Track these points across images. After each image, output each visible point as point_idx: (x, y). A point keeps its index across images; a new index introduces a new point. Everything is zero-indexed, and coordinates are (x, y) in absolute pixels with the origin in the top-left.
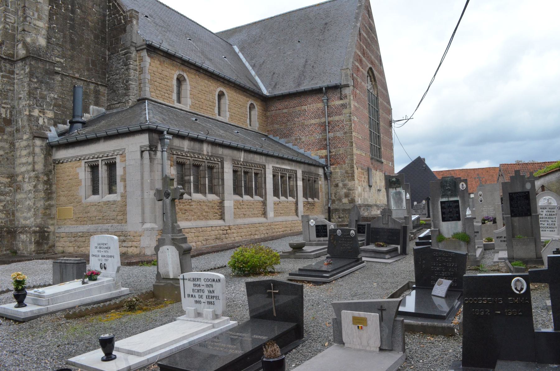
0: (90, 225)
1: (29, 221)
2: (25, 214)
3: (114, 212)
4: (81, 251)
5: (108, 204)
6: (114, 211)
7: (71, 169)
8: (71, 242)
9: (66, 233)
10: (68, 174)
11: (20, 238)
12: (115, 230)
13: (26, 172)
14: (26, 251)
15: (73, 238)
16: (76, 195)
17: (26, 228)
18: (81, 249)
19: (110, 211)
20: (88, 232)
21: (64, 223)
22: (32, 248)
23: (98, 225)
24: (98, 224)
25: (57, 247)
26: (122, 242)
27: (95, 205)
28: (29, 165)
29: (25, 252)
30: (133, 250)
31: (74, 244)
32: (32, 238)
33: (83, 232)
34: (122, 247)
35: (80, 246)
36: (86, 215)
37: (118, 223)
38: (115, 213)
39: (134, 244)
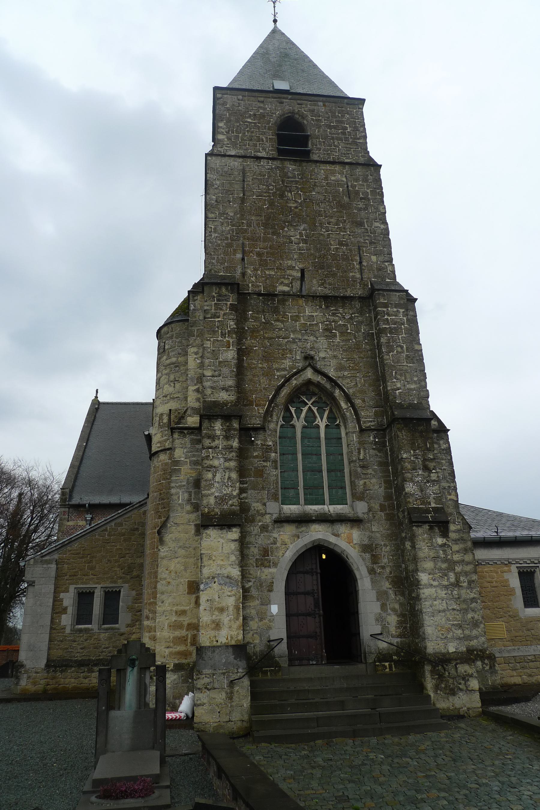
1: (475, 641)
7: (495, 574)
10: (489, 579)
13: (461, 573)
16: (508, 607)
22: (496, 680)
28: (467, 565)
33: (534, 655)
35: (533, 674)
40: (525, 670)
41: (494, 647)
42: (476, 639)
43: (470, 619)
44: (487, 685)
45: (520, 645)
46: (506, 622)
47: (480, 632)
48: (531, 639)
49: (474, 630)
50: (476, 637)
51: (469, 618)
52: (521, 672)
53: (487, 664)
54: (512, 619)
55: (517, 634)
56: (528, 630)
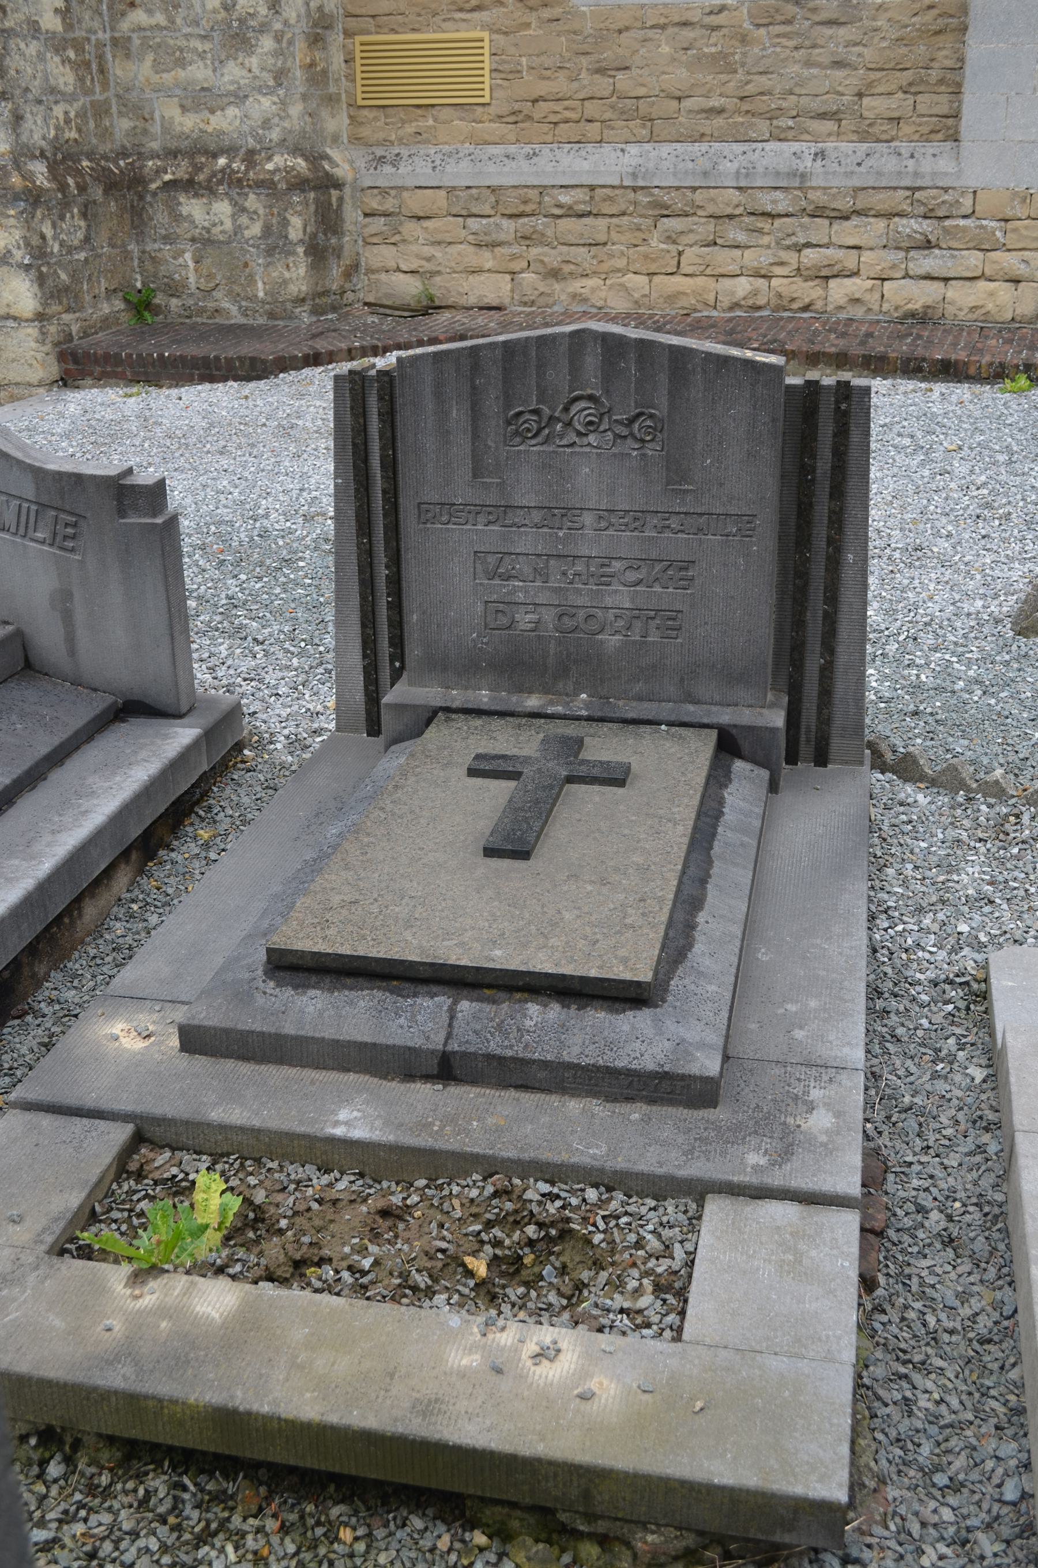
0: (633, 149)
1: (232, 111)
2: (199, 72)
3: (840, 74)
4: (574, 296)
5: (788, 22)
6: (838, 64)
8: (494, 245)
9: (451, 190)
11: (177, 217)
12: (857, 182)
14: (235, 298)
15: (505, 223)
17: (215, 156)
18: (575, 286)
19: (808, 64)
20: (635, 189)
21: (410, 129)
22: (285, 282)
23: (704, 147)
24: (701, 137)
25: (370, 271)
26: (908, 249)
27: (685, 24)
29: (226, 304)
30: (991, 294)
31: (514, 257)
32: (285, 223)
33: (592, 188)
34: (907, 276)
35: (567, 268)
36: (602, 85)
37: (864, 136)
38: (848, 81)
39: (1010, 261)
40: (535, 251)
41: (427, 142)
42: (237, 105)
43: (215, 11)
44: (247, 298)
45: (549, 138)
46: (499, 31)
47: (256, 71)
48: (607, 115)
49: (231, 64)
50: (239, 97)
51: (209, 6)
52: (514, 257)
53: (255, 212)
54: (532, 18)
55: (543, 88)
56: (601, 71)
